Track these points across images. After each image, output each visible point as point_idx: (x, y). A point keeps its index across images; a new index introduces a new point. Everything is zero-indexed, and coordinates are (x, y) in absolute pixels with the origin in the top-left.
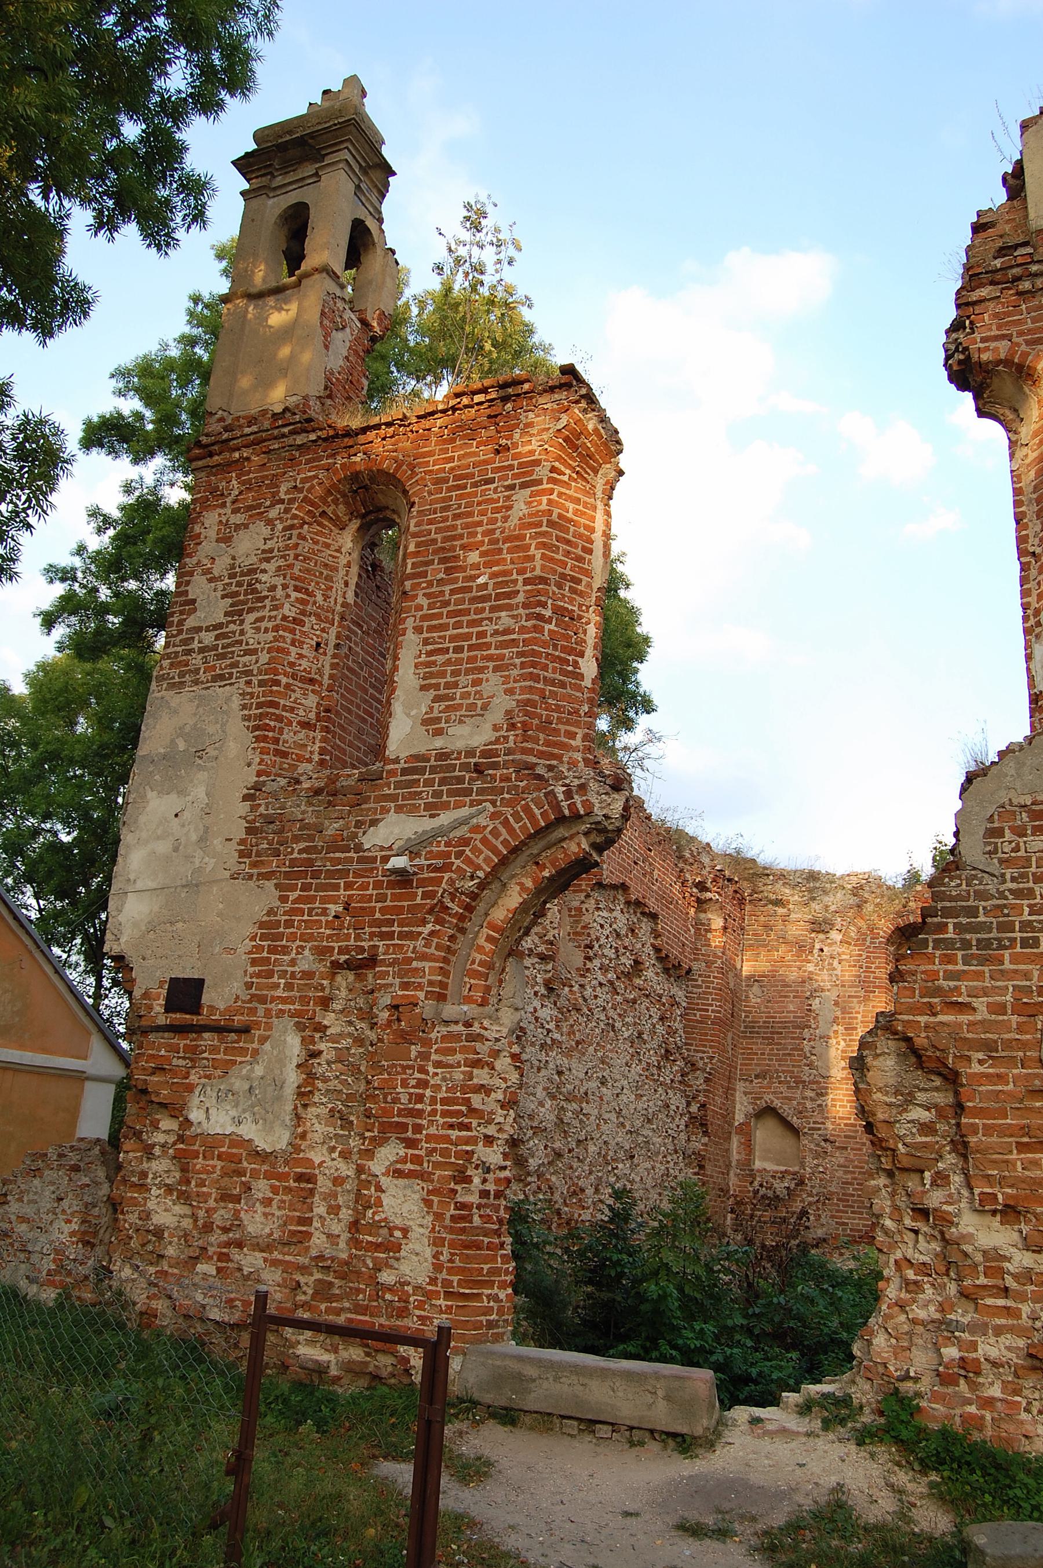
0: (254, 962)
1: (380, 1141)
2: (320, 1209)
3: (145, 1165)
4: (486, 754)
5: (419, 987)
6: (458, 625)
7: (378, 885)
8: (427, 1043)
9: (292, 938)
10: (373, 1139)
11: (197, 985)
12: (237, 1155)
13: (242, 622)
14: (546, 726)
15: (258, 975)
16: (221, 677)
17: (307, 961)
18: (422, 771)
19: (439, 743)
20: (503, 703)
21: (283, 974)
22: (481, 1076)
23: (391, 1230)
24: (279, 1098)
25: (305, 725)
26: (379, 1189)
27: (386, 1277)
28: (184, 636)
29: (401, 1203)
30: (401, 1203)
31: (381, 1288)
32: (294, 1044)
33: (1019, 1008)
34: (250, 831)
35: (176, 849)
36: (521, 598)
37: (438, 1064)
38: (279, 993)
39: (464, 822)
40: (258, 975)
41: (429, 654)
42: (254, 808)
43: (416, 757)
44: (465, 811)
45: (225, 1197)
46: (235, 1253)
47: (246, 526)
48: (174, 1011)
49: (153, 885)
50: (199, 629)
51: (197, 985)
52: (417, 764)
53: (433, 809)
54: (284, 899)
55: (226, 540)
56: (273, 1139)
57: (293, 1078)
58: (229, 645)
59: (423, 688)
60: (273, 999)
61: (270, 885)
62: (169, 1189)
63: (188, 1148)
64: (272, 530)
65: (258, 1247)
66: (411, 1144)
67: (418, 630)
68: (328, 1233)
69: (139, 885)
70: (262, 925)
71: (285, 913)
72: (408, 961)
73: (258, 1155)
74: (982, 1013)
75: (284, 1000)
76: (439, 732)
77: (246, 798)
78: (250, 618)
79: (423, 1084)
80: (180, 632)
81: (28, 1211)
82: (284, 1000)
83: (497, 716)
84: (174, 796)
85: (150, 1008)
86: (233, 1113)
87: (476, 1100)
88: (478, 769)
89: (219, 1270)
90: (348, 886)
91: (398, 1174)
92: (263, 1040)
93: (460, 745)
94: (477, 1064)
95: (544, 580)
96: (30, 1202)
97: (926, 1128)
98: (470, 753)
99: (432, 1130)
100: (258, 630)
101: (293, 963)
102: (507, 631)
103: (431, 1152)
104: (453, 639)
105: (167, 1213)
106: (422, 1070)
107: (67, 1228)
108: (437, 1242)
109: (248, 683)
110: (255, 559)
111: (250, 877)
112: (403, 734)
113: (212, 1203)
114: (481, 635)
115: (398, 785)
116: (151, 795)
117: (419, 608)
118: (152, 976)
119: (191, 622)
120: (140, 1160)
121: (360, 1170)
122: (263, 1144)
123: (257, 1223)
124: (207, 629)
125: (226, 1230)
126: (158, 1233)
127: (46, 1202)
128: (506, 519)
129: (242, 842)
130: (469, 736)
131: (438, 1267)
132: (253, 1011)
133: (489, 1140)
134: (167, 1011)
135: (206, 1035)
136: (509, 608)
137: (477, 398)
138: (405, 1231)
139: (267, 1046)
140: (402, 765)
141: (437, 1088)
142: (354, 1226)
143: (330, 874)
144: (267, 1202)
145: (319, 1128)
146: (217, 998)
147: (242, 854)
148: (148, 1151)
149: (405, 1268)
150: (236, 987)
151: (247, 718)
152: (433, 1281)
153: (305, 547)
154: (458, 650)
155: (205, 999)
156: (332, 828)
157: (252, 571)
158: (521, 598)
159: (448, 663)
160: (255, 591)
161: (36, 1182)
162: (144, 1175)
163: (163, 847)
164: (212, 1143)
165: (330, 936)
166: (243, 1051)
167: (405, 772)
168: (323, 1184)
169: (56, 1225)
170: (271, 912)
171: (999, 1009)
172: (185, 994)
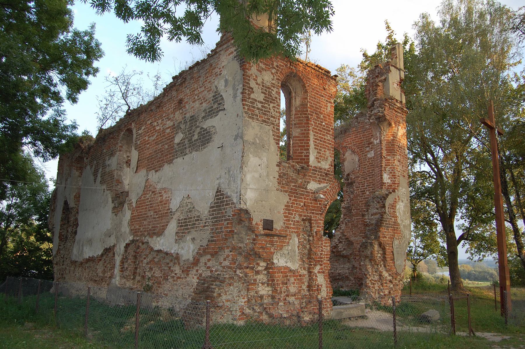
0: (285, 217)
1: (315, 265)
3: (255, 277)
5: (320, 227)
6: (320, 134)
7: (310, 200)
8: (322, 241)
9: (293, 211)
10: (314, 264)
12: (287, 272)
13: (269, 105)
15: (286, 220)
16: (265, 122)
17: (297, 218)
18: (316, 171)
19: (319, 165)
21: (292, 221)
23: (318, 286)
24: (295, 255)
26: (316, 276)
28: (251, 100)
34: (280, 176)
35: (260, 177)
36: (331, 133)
37: (324, 246)
38: (292, 226)
40: (286, 220)
41: (316, 139)
42: (280, 169)
43: (315, 167)
44: (325, 185)
46: (287, 298)
47: (266, 71)
48: (266, 229)
49: (255, 187)
50: (256, 100)
52: (315, 169)
53: (320, 182)
54: (290, 199)
58: (266, 111)
59: (315, 148)
60: (291, 228)
61: (287, 194)
62: (263, 284)
64: (274, 77)
65: (292, 296)
66: (321, 265)
67: (313, 131)
69: (251, 186)
70: (286, 206)
71: (291, 203)
72: (318, 220)
73: (291, 271)
74: (388, 239)
75: (293, 228)
76: (319, 162)
77: (277, 165)
78: (272, 105)
79: (322, 251)
80: (249, 98)
81: (229, 297)
82: (293, 228)
84: (257, 158)
85: (258, 228)
86: (285, 260)
88: (326, 174)
89: (284, 303)
90: (305, 199)
91: (319, 272)
92: (290, 239)
93: (323, 167)
96: (229, 294)
97: (380, 257)
98: (325, 170)
99: (325, 262)
100: (274, 110)
101: (294, 218)
102: (329, 140)
103: (325, 267)
104: (320, 137)
106: (322, 248)
107: (243, 301)
109: (274, 127)
110: (269, 84)
111: (282, 191)
113: (281, 286)
114: (325, 139)
115: (312, 173)
116: (250, 155)
117: (312, 125)
119: (252, 96)
120: (253, 276)
121: (310, 272)
124: (258, 102)
125: (284, 292)
126: (261, 297)
128: (327, 109)
129: (278, 179)
131: (327, 293)
132: (286, 231)
134: (264, 229)
135: (275, 237)
136: (329, 134)
137: (320, 70)
138: (321, 285)
139: (291, 241)
140: (312, 168)
141: (325, 252)
143: (301, 194)
144: (294, 283)
146: (278, 226)
147: (279, 183)
149: (322, 294)
150: (281, 223)
151: (274, 139)
152: (327, 296)
154: (321, 141)
155: (275, 226)
158: (331, 133)
159: (319, 143)
160: (271, 96)
161: (232, 287)
162: (255, 280)
163: (257, 175)
164: (279, 268)
165: (301, 212)
166: (284, 242)
167: (313, 170)
169: (240, 300)
170: (288, 202)
172: (268, 224)
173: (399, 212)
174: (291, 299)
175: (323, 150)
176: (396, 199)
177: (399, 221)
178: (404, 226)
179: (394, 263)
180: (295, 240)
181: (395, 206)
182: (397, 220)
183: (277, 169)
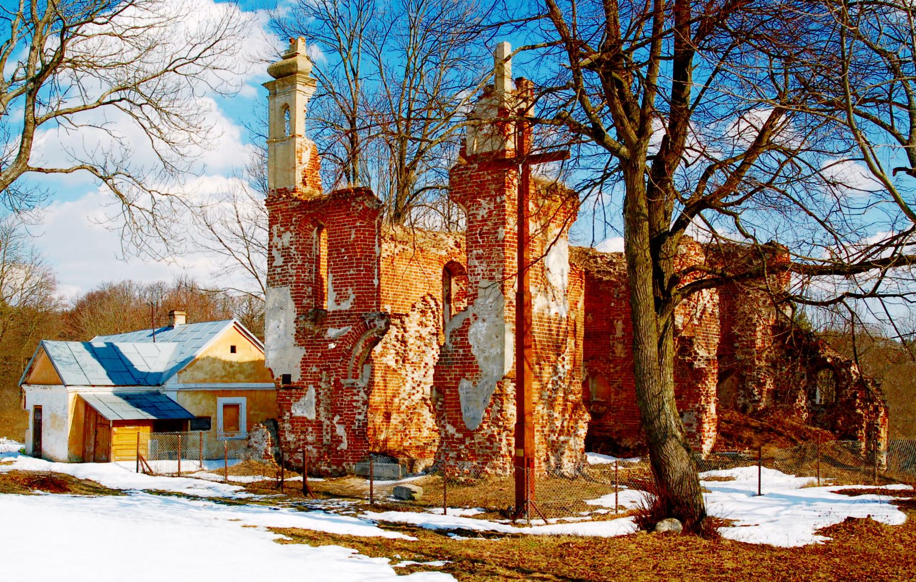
1: (334, 416)
2: (324, 433)
4: (350, 311)
11: (290, 376)
12: (303, 421)
14: (364, 303)
19: (339, 308)
20: (353, 296)
22: (356, 398)
25: (309, 297)
27: (338, 449)
29: (340, 431)
30: (340, 431)
31: (338, 451)
32: (313, 390)
33: (455, 379)
39: (345, 331)
45: (302, 432)
51: (290, 376)
53: (339, 326)
55: (279, 236)
56: (312, 417)
57: (314, 400)
63: (293, 420)
66: (341, 416)
68: (326, 438)
76: (339, 304)
78: (290, 264)
81: (256, 440)
83: (351, 300)
87: (354, 404)
88: (349, 315)
91: (338, 423)
94: (355, 395)
95: (361, 259)
105: (290, 438)
108: (348, 439)
112: (329, 305)
118: (278, 374)
122: (309, 418)
123: (310, 438)
126: (289, 442)
127: (260, 437)
130: (346, 306)
133: (360, 414)
142: (332, 437)
145: (323, 413)
146: (295, 379)
148: (284, 421)
150: (299, 377)
153: (302, 240)
155: (292, 380)
156: (317, 331)
157: (288, 248)
163: (276, 336)
168: (325, 427)
171: (451, 379)
172: (287, 378)
173: (476, 338)
174: (310, 447)
175: (344, 289)
176: (468, 319)
177: (474, 351)
178: (486, 358)
179: (461, 414)
180: (312, 391)
181: (467, 331)
182: (469, 351)
183: (295, 325)
